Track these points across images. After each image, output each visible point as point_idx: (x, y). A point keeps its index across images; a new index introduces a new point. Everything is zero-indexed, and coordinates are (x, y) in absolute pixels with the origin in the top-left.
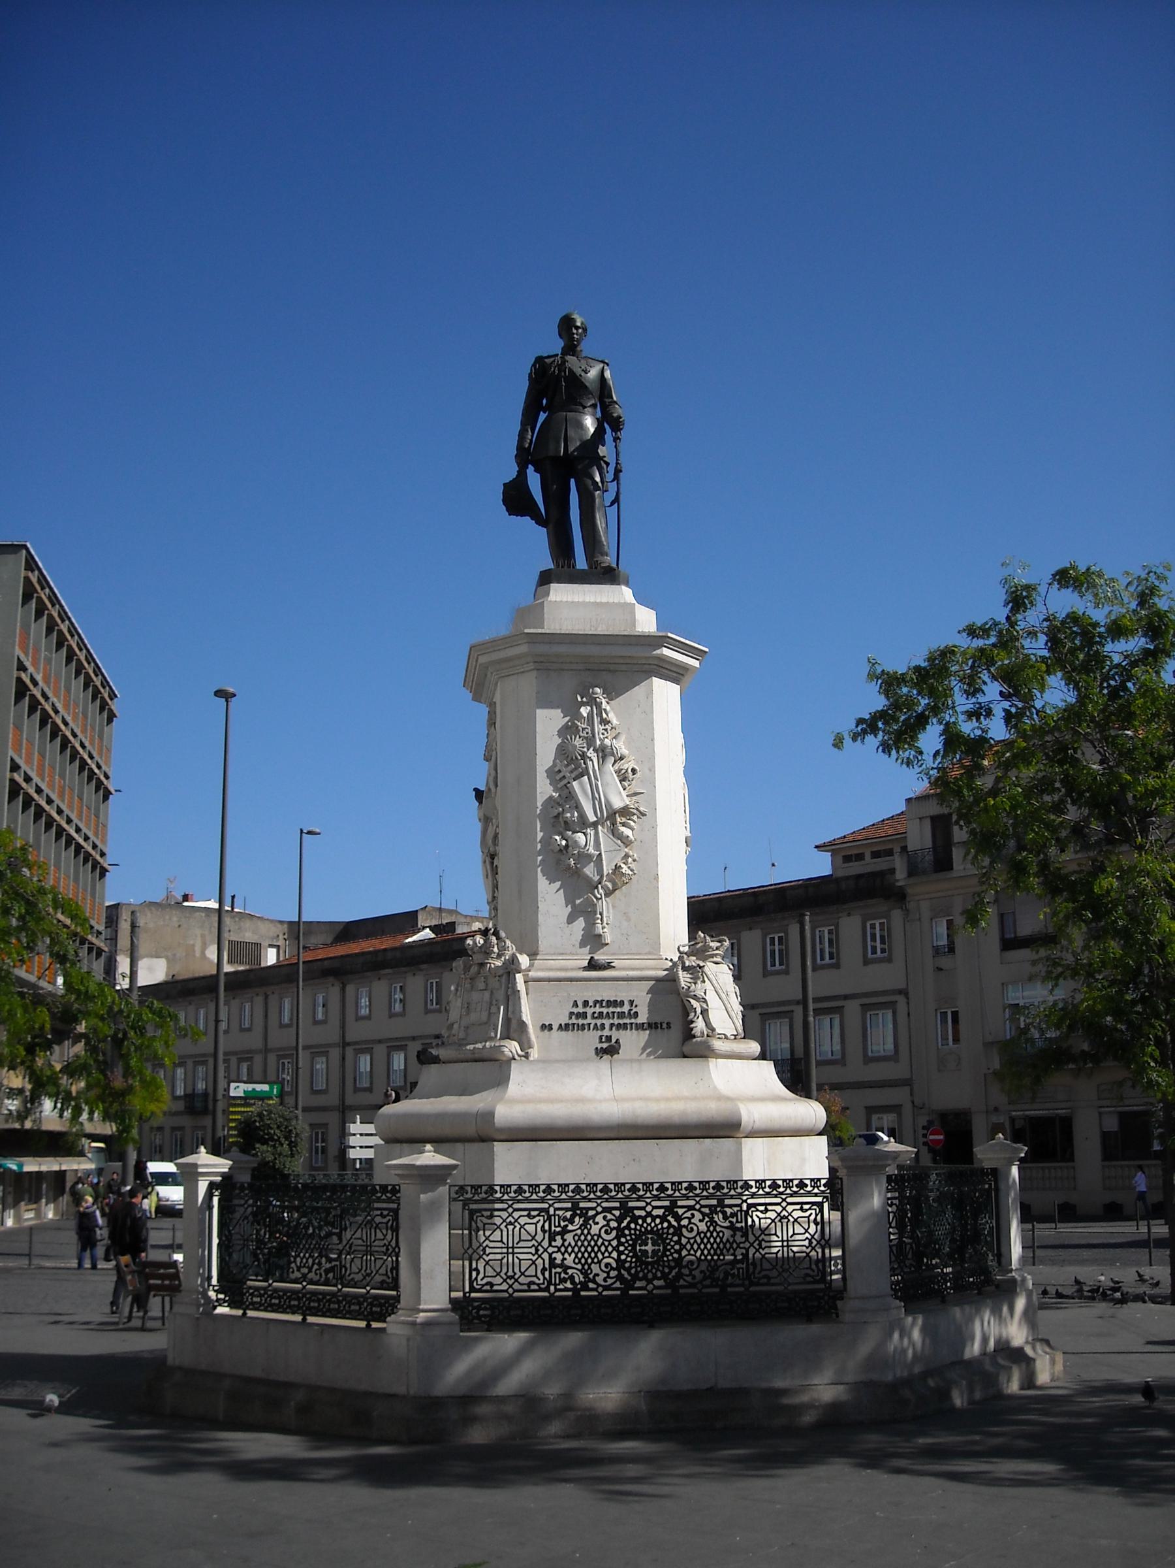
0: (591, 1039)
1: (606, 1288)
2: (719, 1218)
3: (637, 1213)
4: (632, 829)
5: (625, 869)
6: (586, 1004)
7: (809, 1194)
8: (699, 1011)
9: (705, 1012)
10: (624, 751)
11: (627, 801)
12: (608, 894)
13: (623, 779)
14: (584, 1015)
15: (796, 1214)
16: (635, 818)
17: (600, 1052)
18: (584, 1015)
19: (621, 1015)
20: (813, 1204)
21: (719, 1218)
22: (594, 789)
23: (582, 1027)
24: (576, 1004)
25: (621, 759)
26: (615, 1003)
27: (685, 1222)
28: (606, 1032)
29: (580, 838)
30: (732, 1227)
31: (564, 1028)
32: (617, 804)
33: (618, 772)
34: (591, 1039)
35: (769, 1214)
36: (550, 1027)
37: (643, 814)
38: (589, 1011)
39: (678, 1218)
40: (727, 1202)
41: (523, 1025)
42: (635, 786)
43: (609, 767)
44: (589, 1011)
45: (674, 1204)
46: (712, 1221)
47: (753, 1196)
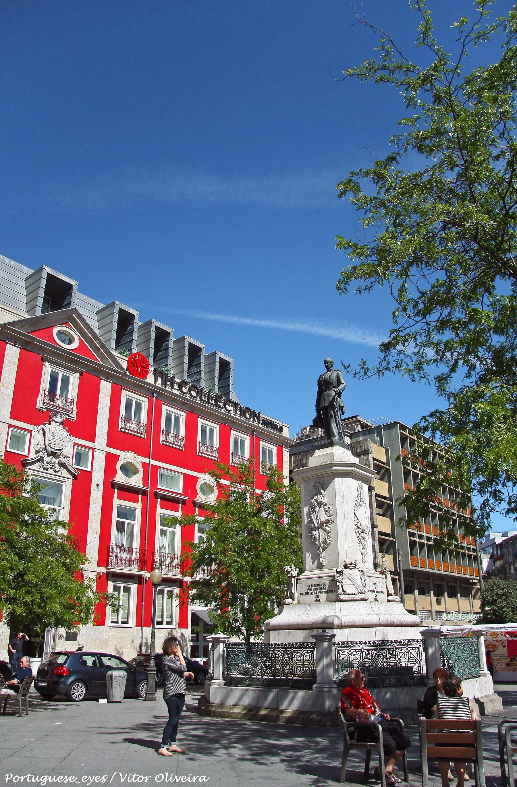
0: (313, 597)
1: (258, 675)
2: (285, 655)
3: (266, 652)
4: (330, 528)
5: (328, 541)
6: (312, 586)
7: (310, 647)
8: (340, 586)
9: (342, 586)
10: (327, 502)
11: (327, 518)
12: (324, 550)
13: (326, 511)
14: (311, 589)
15: (411, 651)
16: (330, 523)
17: (316, 601)
18: (311, 589)
19: (321, 589)
20: (311, 651)
21: (285, 655)
22: (317, 516)
23: (311, 593)
24: (309, 586)
25: (326, 505)
26: (319, 585)
27: (277, 656)
28: (318, 595)
29: (314, 533)
30: (289, 658)
31: (307, 594)
32: (323, 520)
33: (324, 509)
34: (313, 597)
35: (402, 651)
36: (302, 594)
37: (333, 522)
38: (313, 588)
39: (275, 655)
40: (288, 650)
41: (293, 595)
42: (331, 513)
43: (322, 508)
44: (313, 588)
45: (274, 650)
46: (284, 655)
47: (295, 648)
